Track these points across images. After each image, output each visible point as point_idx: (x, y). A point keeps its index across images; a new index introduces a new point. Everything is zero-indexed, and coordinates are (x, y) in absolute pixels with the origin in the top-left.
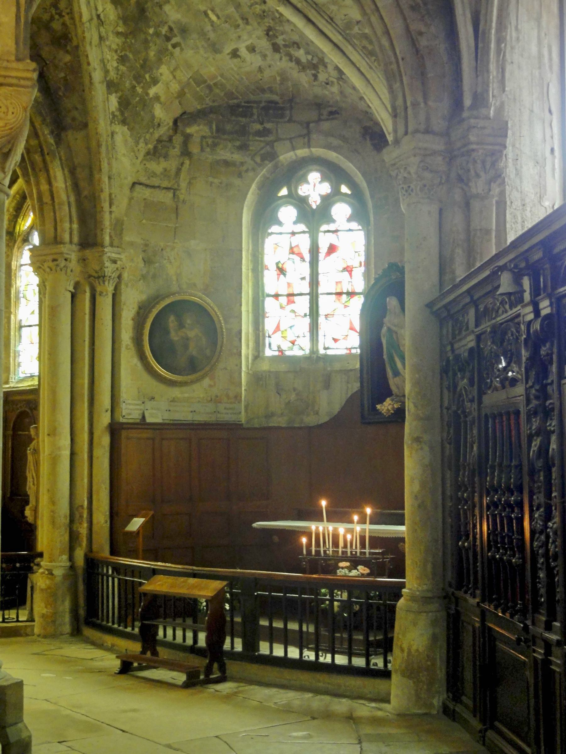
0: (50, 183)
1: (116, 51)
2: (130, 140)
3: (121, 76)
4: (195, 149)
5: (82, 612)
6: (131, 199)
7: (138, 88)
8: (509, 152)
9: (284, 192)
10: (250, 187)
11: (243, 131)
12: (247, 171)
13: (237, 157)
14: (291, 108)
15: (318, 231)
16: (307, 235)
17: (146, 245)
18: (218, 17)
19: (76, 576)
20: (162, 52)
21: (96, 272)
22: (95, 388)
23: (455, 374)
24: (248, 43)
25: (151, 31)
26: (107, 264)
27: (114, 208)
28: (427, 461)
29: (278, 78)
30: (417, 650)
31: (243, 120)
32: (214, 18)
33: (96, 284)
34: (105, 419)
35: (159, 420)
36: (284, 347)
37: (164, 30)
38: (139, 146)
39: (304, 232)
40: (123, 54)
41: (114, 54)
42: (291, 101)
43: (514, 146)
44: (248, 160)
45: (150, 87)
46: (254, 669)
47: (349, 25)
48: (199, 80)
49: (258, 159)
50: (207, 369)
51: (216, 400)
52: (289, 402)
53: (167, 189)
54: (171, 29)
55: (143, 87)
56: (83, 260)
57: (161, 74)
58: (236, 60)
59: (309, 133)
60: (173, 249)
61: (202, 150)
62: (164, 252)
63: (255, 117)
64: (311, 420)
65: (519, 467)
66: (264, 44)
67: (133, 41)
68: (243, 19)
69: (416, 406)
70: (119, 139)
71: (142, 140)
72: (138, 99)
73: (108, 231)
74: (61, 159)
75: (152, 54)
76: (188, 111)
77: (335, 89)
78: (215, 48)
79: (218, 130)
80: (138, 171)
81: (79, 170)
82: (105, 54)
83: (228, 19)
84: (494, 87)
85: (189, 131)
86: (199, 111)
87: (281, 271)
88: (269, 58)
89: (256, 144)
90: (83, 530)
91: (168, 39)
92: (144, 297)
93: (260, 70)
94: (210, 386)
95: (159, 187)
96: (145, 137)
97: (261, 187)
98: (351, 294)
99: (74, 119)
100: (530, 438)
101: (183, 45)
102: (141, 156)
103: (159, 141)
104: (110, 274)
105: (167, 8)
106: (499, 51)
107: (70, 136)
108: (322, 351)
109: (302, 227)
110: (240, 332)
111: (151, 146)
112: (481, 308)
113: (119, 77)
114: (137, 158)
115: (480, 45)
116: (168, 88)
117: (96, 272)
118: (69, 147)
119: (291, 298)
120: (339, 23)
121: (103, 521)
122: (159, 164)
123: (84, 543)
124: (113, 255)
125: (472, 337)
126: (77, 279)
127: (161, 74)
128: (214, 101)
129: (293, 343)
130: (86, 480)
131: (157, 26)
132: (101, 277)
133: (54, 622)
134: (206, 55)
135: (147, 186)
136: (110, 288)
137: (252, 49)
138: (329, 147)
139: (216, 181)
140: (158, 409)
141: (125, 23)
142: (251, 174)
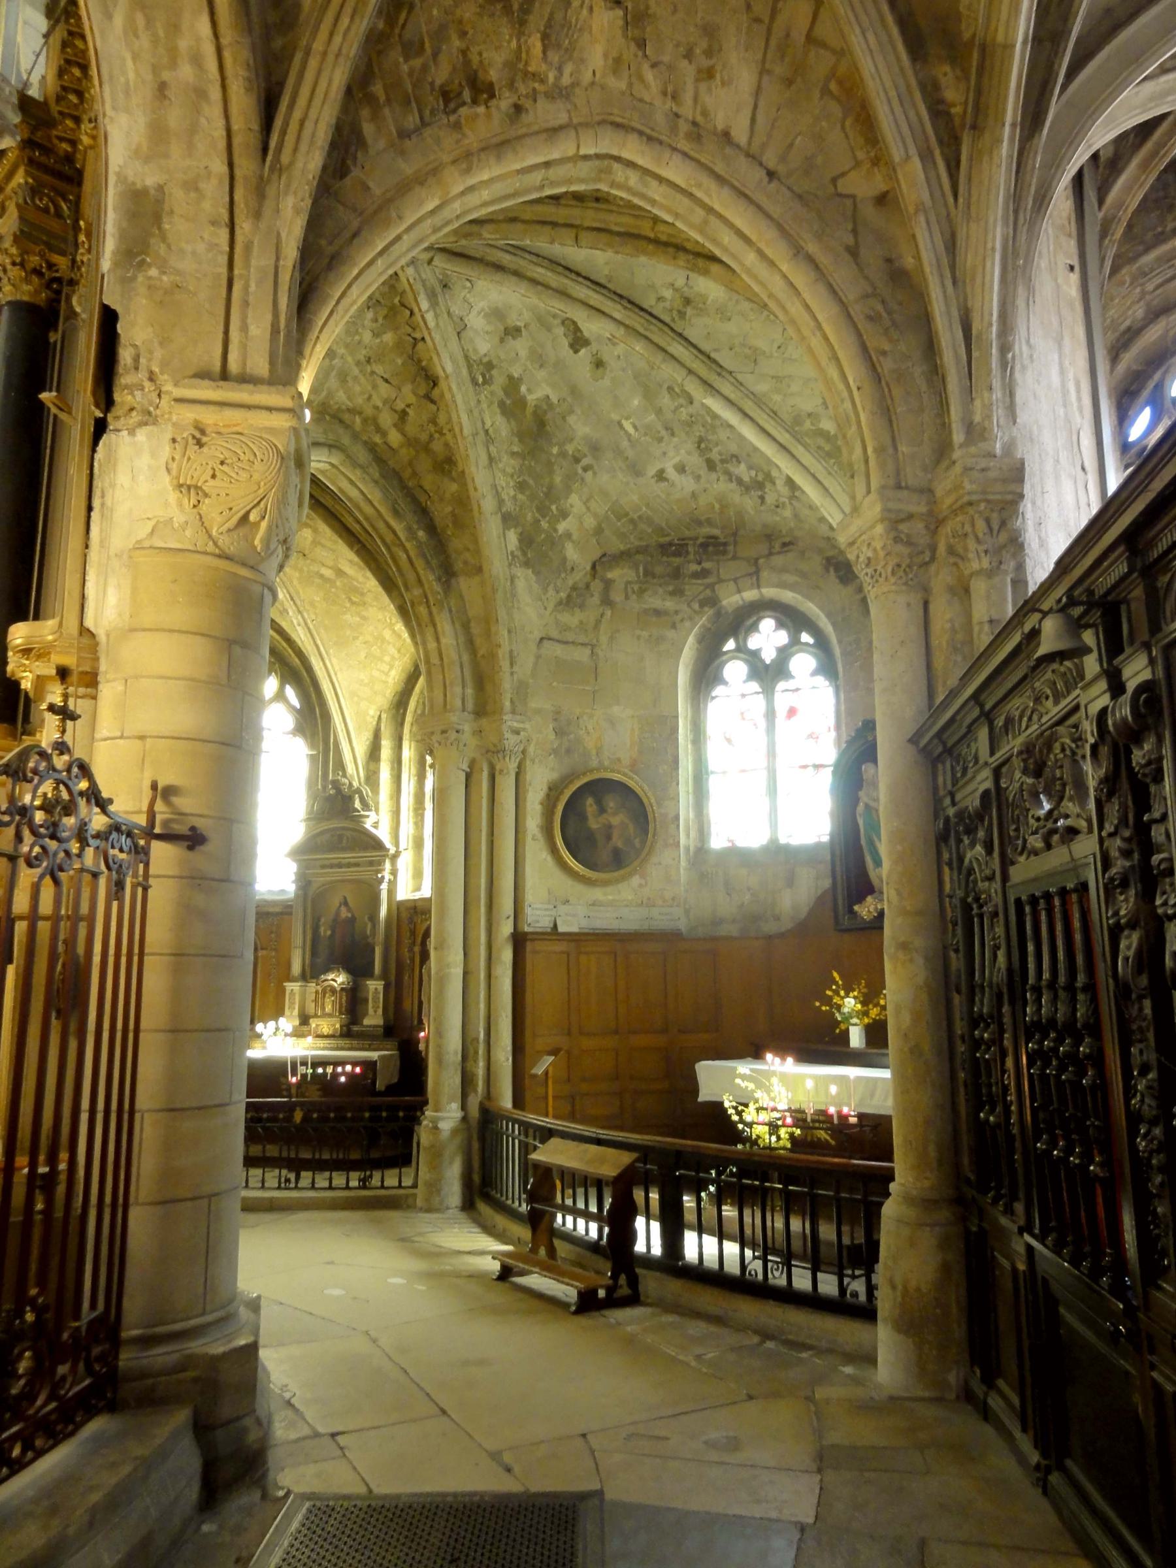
0: (438, 640)
1: (512, 476)
2: (535, 586)
3: (521, 507)
4: (617, 596)
5: (476, 1178)
6: (538, 657)
7: (542, 523)
8: (1027, 507)
9: (730, 645)
12: (682, 620)
13: (669, 604)
17: (558, 713)
20: (570, 478)
23: (959, 841)
24: (677, 460)
25: (555, 450)
26: (507, 735)
27: (516, 669)
28: (921, 979)
29: (717, 506)
30: (918, 1289)
31: (677, 561)
32: (631, 430)
33: (495, 760)
34: (507, 929)
35: (575, 929)
37: (570, 449)
40: (521, 479)
41: (509, 479)
42: (735, 534)
43: (1034, 503)
44: (685, 607)
46: (674, 1287)
47: (798, 420)
49: (696, 606)
51: (649, 904)
52: (743, 904)
55: (549, 522)
56: (479, 732)
58: (664, 485)
59: (757, 573)
60: (591, 716)
61: (627, 597)
62: (581, 721)
63: (691, 557)
64: (770, 928)
65: (1091, 988)
66: (695, 461)
68: (667, 429)
69: (899, 893)
70: (521, 584)
72: (543, 536)
73: (509, 696)
74: (450, 611)
75: (558, 479)
77: (787, 513)
78: (635, 470)
81: (472, 624)
84: (999, 414)
85: (610, 575)
86: (622, 553)
87: (729, 741)
88: (703, 480)
89: (694, 588)
90: (480, 1071)
91: (577, 460)
92: (555, 776)
93: (694, 495)
94: (641, 886)
97: (700, 640)
98: (817, 767)
99: (466, 563)
100: (1116, 932)
102: (551, 606)
103: (574, 588)
105: (572, 419)
106: (1004, 364)
107: (466, 585)
108: (783, 840)
109: (754, 686)
110: (677, 818)
111: (563, 595)
112: (1000, 722)
114: (546, 608)
115: (975, 354)
117: (495, 746)
118: (462, 597)
120: (785, 417)
124: (515, 724)
125: (986, 773)
127: (572, 506)
128: (641, 539)
131: (561, 445)
135: (558, 641)
136: (512, 766)
137: (681, 469)
138: (783, 585)
139: (645, 634)
140: (574, 916)
142: (687, 624)
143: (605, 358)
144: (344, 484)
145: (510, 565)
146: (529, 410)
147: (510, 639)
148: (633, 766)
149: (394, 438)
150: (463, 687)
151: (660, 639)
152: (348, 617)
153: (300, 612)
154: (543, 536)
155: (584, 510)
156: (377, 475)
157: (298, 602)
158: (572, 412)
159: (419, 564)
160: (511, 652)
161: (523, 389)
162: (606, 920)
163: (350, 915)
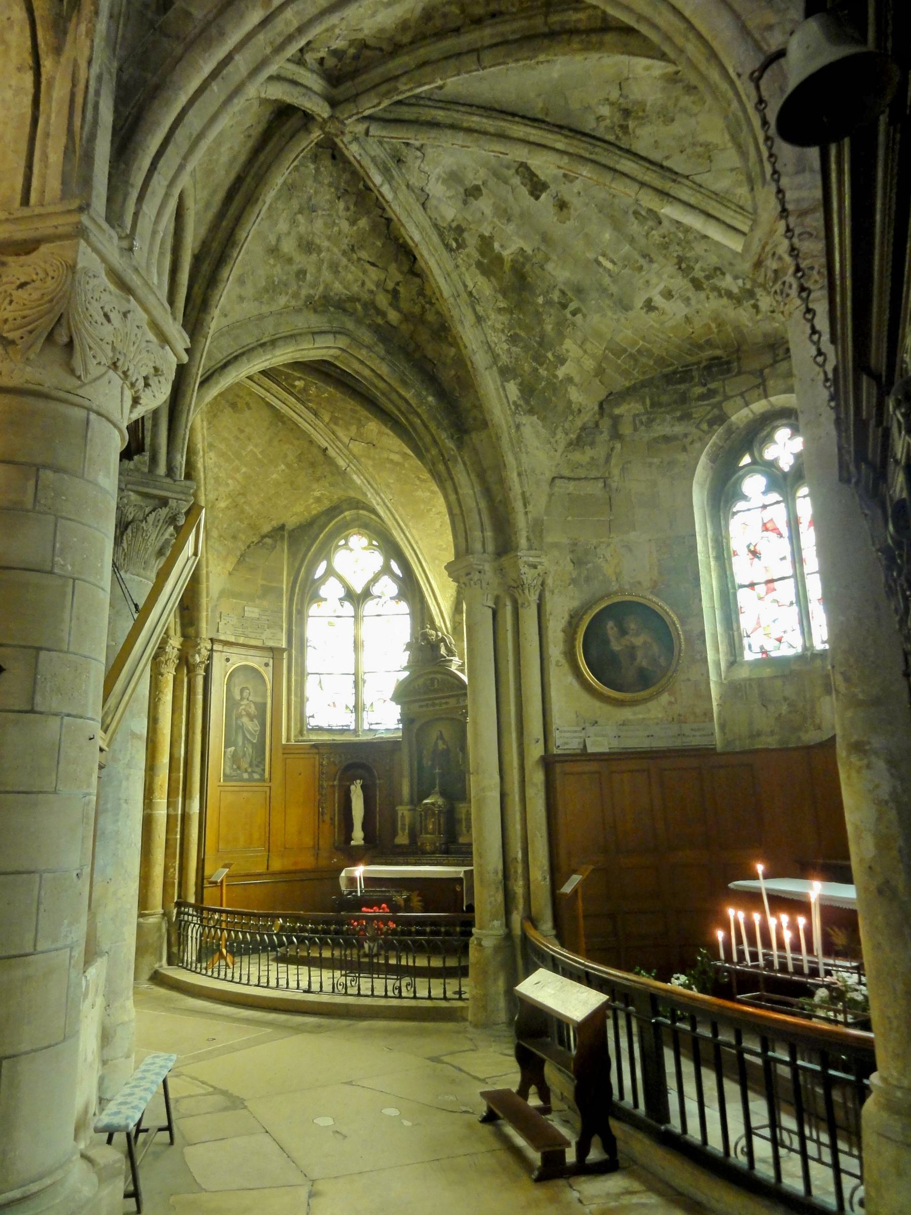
0: (457, 493)
1: (503, 331)
3: (517, 359)
4: (626, 429)
6: (551, 495)
7: (541, 371)
9: (746, 460)
10: (697, 460)
11: (683, 399)
12: (692, 442)
13: (679, 429)
14: (739, 359)
15: (794, 499)
16: (783, 505)
17: (575, 544)
18: (614, 263)
19: (512, 947)
20: (560, 325)
21: (515, 581)
22: (524, 714)
24: (661, 286)
25: (540, 300)
26: (525, 569)
28: (884, 791)
29: (713, 325)
31: (682, 387)
32: (609, 265)
33: (517, 595)
34: (536, 751)
35: (605, 749)
36: (767, 648)
37: (555, 296)
38: (558, 437)
39: (778, 502)
40: (512, 332)
41: (500, 334)
42: (738, 350)
44: (694, 430)
45: (556, 367)
48: (619, 351)
49: (705, 426)
50: (663, 681)
51: (680, 720)
52: (780, 715)
53: (596, 479)
54: (563, 293)
55: (547, 369)
56: (501, 571)
58: (653, 315)
59: (763, 384)
60: (609, 545)
61: (636, 429)
62: (598, 550)
63: (696, 380)
66: (680, 283)
67: (521, 316)
68: (644, 256)
69: (847, 680)
70: (527, 431)
71: (560, 429)
72: (543, 383)
74: (465, 464)
75: (549, 328)
76: (614, 391)
78: (624, 306)
79: (653, 405)
80: (558, 464)
81: (489, 473)
82: (489, 336)
83: (627, 261)
85: (617, 411)
86: (628, 389)
87: (755, 554)
88: (693, 302)
89: (701, 410)
91: (564, 306)
92: (576, 604)
93: (687, 319)
94: (670, 703)
95: (585, 478)
96: (563, 427)
97: (713, 459)
99: (475, 419)
101: (584, 310)
102: (561, 447)
103: (583, 428)
104: (529, 582)
105: (550, 267)
107: (476, 438)
109: (775, 496)
110: (703, 633)
111: (573, 436)
113: (513, 361)
114: (556, 451)
116: (581, 366)
117: (515, 581)
119: (771, 585)
121: (540, 878)
122: (584, 453)
123: (521, 906)
124: (531, 559)
126: (496, 593)
127: (568, 351)
128: (644, 373)
129: (779, 640)
130: (518, 827)
131: (546, 293)
132: (520, 585)
133: (485, 1007)
134: (615, 317)
135: (569, 479)
136: (533, 598)
137: (668, 295)
139: (656, 460)
140: (603, 736)
141: (505, 295)
142: (697, 445)
143: (567, 198)
144: (357, 366)
145: (514, 414)
146: (507, 266)
147: (521, 482)
148: (655, 588)
149: (393, 316)
150: (482, 532)
151: (672, 464)
152: (419, 493)
153: (378, 494)
154: (543, 383)
155: (581, 352)
156: (382, 353)
157: (375, 486)
158: (548, 259)
159: (432, 426)
160: (523, 494)
161: (496, 245)
162: (637, 741)
163: (445, 747)
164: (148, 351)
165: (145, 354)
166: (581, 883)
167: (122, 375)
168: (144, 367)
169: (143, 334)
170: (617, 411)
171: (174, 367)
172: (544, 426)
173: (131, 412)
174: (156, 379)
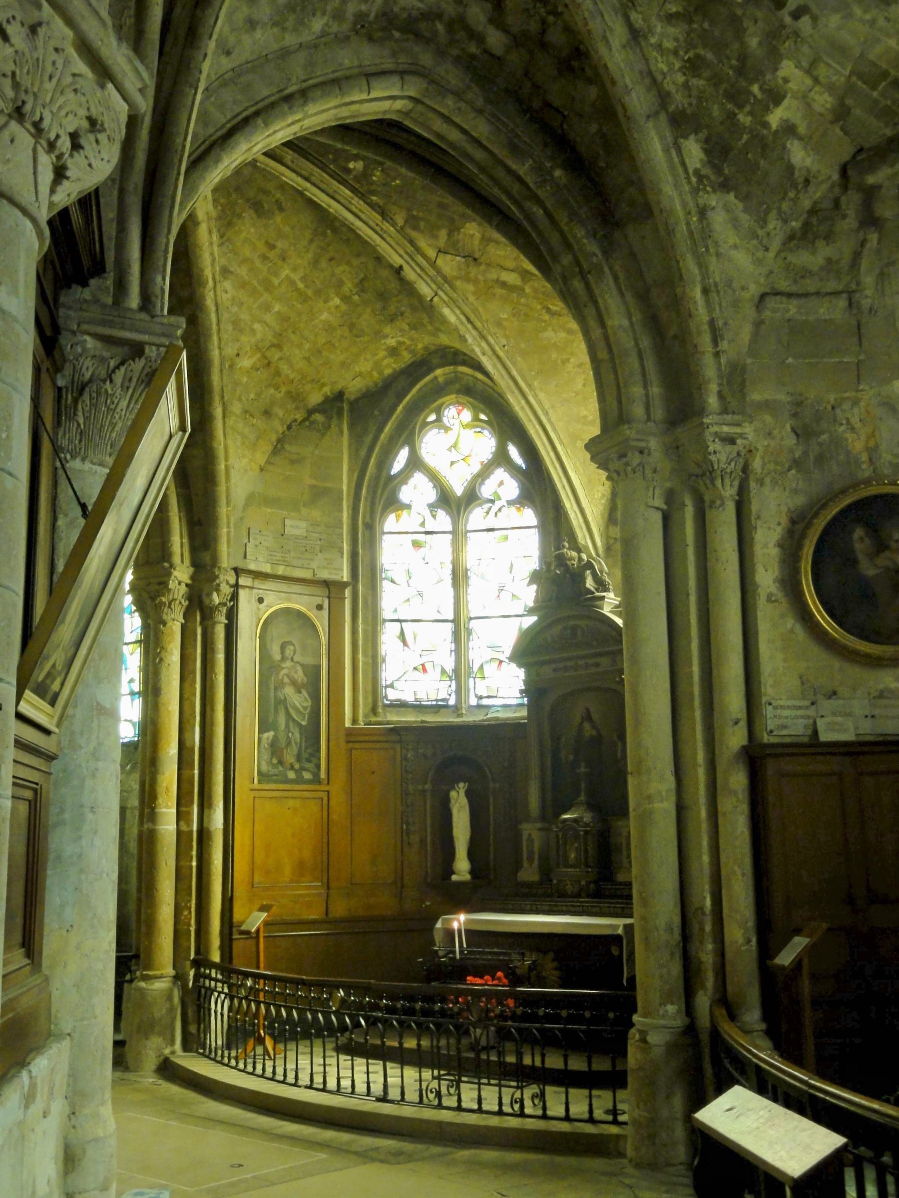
0: (603, 324)
1: (676, 53)
2: (745, 219)
3: (700, 98)
6: (758, 324)
17: (799, 404)
19: (696, 1044)
21: (699, 466)
26: (714, 446)
27: (724, 345)
33: (702, 488)
38: (771, 226)
40: (691, 54)
41: (672, 59)
45: (767, 110)
53: (836, 294)
55: (751, 113)
56: (674, 450)
57: (786, 80)
60: (856, 403)
62: (838, 411)
67: (706, 25)
70: (718, 220)
71: (773, 214)
72: (745, 137)
73: (714, 387)
74: (616, 278)
75: (753, 42)
76: (867, 146)
80: (771, 272)
82: (652, 62)
85: (871, 180)
92: (800, 501)
95: (817, 293)
96: (779, 209)
101: (815, 9)
102: (776, 245)
103: (813, 212)
104: (722, 466)
113: (694, 102)
114: (767, 249)
116: (809, 105)
118: (633, 255)
121: (741, 941)
122: (814, 253)
124: (726, 429)
126: (668, 485)
127: (786, 80)
130: (706, 859)
133: (652, 1137)
134: (868, 17)
135: (790, 295)
136: (729, 492)
140: (849, 715)
144: (439, 125)
145: (695, 191)
147: (709, 304)
149: (495, 39)
150: (645, 387)
152: (549, 334)
153: (483, 337)
154: (745, 137)
155: (809, 82)
156: (480, 102)
157: (479, 325)
159: (562, 217)
163: (594, 733)
164: (75, 91)
165: (71, 95)
166: (810, 950)
167: (32, 130)
168: (71, 117)
169: (67, 62)
170: (871, 180)
171: (124, 119)
172: (746, 210)
173: (53, 191)
174: (91, 137)
